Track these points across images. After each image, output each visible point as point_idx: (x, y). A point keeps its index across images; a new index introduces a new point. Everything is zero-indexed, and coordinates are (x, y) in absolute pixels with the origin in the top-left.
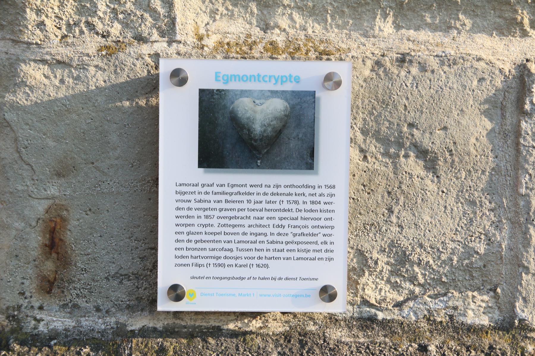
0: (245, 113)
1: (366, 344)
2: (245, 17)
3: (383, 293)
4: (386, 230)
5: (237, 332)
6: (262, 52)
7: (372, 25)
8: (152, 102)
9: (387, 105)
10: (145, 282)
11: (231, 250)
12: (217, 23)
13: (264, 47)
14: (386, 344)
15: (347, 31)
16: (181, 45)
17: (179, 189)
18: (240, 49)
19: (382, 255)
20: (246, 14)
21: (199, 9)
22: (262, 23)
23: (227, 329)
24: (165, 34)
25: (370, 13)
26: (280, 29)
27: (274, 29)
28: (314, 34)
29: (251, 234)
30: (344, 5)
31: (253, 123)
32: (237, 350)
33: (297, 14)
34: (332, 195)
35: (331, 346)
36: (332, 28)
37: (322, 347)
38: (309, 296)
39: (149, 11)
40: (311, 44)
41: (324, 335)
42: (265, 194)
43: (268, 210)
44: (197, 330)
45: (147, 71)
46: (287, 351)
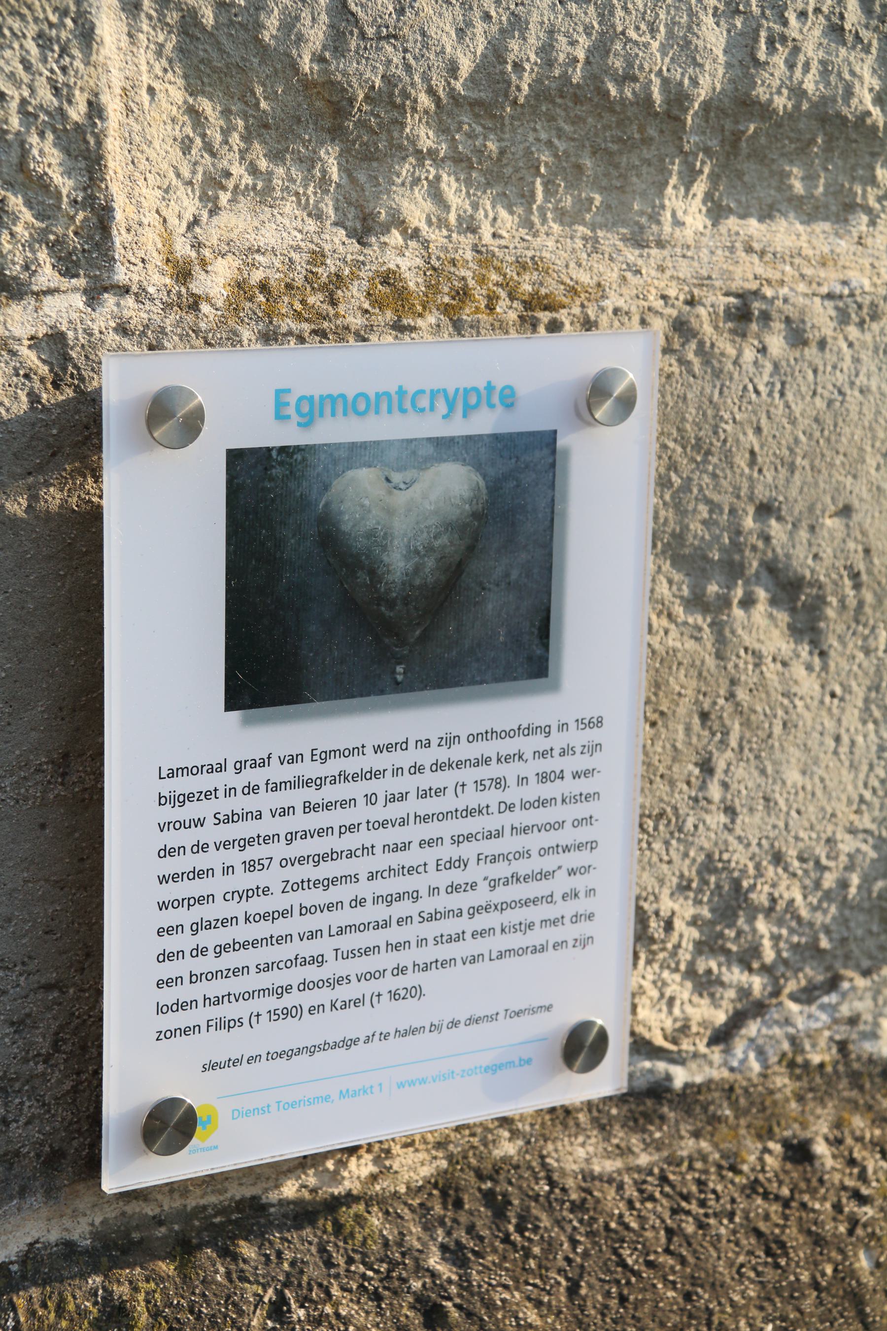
0: (363, 518)
1: (656, 1171)
2: (305, 194)
3: (677, 1011)
4: (696, 827)
5: (309, 1203)
6: (366, 311)
7: (654, 207)
8: (46, 501)
9: (708, 453)
10: (29, 1099)
11: (320, 959)
12: (224, 218)
13: (369, 294)
14: (704, 1158)
15: (585, 229)
16: (130, 301)
17: (169, 786)
18: (303, 302)
19: (681, 900)
20: (306, 187)
21: (172, 175)
22: (352, 213)
23: (283, 1203)
24: (77, 264)
25: (652, 170)
26: (404, 232)
27: (388, 231)
28: (498, 242)
29: (375, 901)
30: (584, 146)
31: (384, 548)
32: (329, 1263)
33: (452, 178)
34: (593, 748)
35: (574, 1196)
36: (544, 220)
37: (550, 1203)
38: (529, 1061)
39: (23, 184)
40: (494, 277)
41: (544, 1165)
42: (417, 769)
43: (425, 819)
44: (197, 1223)
45: (28, 395)
46: (461, 1235)
